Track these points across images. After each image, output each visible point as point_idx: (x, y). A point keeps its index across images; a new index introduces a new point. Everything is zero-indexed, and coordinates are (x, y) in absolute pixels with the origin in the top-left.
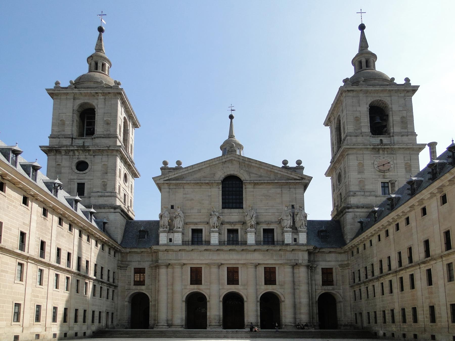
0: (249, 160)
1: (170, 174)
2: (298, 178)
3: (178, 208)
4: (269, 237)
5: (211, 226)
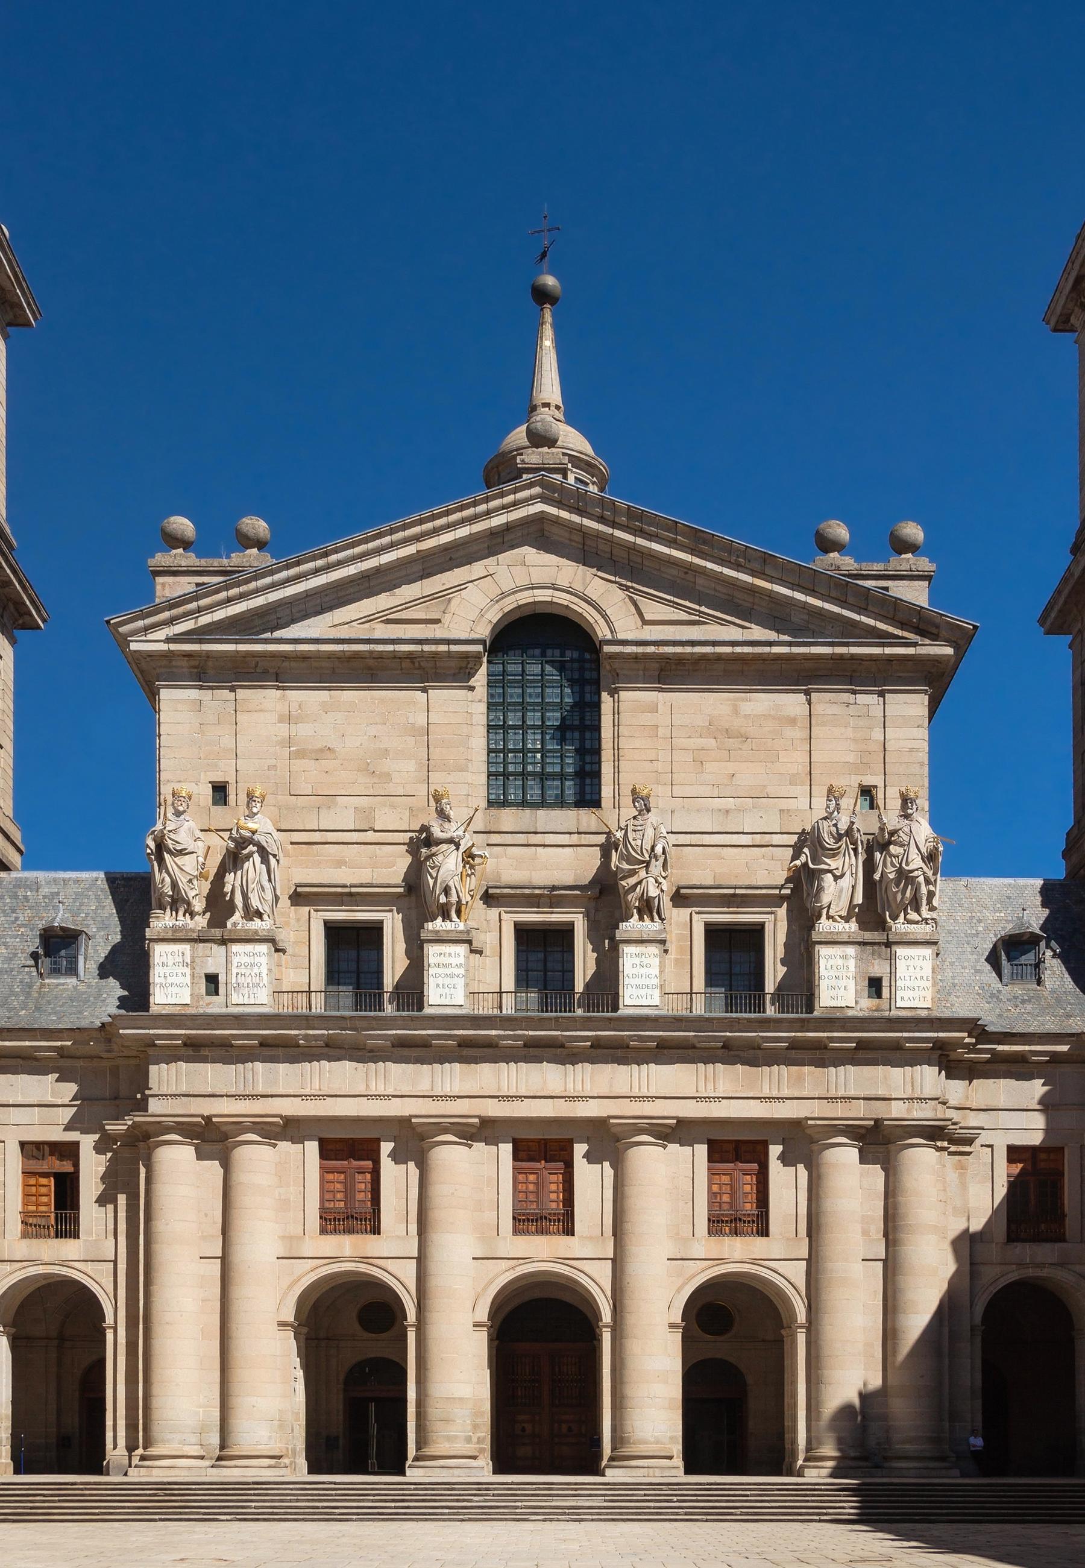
4: (736, 969)
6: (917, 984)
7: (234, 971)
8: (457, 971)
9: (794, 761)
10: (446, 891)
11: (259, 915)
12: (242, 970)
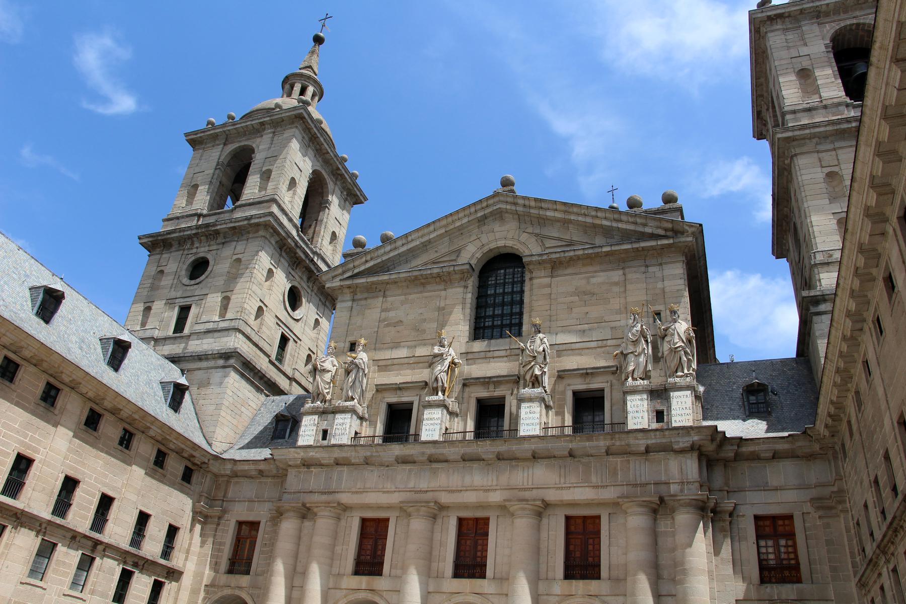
1: (357, 263)
2: (662, 232)
6: (683, 412)
8: (436, 422)
9: (616, 303)
10: (436, 379)
11: (353, 399)
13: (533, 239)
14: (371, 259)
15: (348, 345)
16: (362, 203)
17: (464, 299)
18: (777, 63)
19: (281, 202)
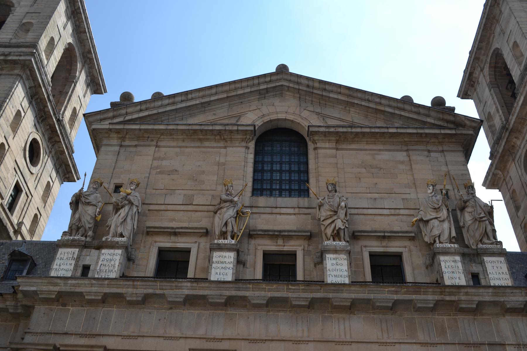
0: (322, 86)
1: (130, 110)
2: (446, 125)
3: (131, 183)
5: (217, 232)
6: (501, 276)
7: (100, 263)
10: (226, 224)
11: (121, 235)
12: (105, 263)
13: (316, 116)
14: (147, 109)
15: (112, 187)
16: (101, 93)
17: (246, 158)
18: (518, 19)
19: (40, 52)
